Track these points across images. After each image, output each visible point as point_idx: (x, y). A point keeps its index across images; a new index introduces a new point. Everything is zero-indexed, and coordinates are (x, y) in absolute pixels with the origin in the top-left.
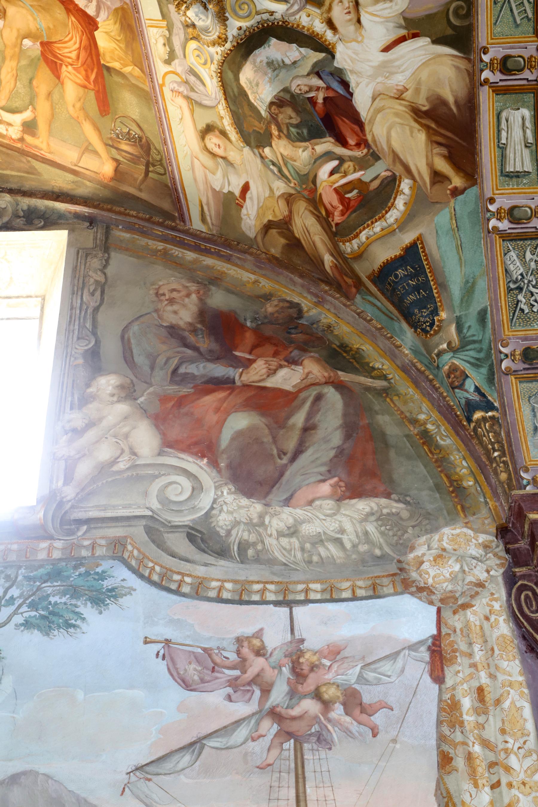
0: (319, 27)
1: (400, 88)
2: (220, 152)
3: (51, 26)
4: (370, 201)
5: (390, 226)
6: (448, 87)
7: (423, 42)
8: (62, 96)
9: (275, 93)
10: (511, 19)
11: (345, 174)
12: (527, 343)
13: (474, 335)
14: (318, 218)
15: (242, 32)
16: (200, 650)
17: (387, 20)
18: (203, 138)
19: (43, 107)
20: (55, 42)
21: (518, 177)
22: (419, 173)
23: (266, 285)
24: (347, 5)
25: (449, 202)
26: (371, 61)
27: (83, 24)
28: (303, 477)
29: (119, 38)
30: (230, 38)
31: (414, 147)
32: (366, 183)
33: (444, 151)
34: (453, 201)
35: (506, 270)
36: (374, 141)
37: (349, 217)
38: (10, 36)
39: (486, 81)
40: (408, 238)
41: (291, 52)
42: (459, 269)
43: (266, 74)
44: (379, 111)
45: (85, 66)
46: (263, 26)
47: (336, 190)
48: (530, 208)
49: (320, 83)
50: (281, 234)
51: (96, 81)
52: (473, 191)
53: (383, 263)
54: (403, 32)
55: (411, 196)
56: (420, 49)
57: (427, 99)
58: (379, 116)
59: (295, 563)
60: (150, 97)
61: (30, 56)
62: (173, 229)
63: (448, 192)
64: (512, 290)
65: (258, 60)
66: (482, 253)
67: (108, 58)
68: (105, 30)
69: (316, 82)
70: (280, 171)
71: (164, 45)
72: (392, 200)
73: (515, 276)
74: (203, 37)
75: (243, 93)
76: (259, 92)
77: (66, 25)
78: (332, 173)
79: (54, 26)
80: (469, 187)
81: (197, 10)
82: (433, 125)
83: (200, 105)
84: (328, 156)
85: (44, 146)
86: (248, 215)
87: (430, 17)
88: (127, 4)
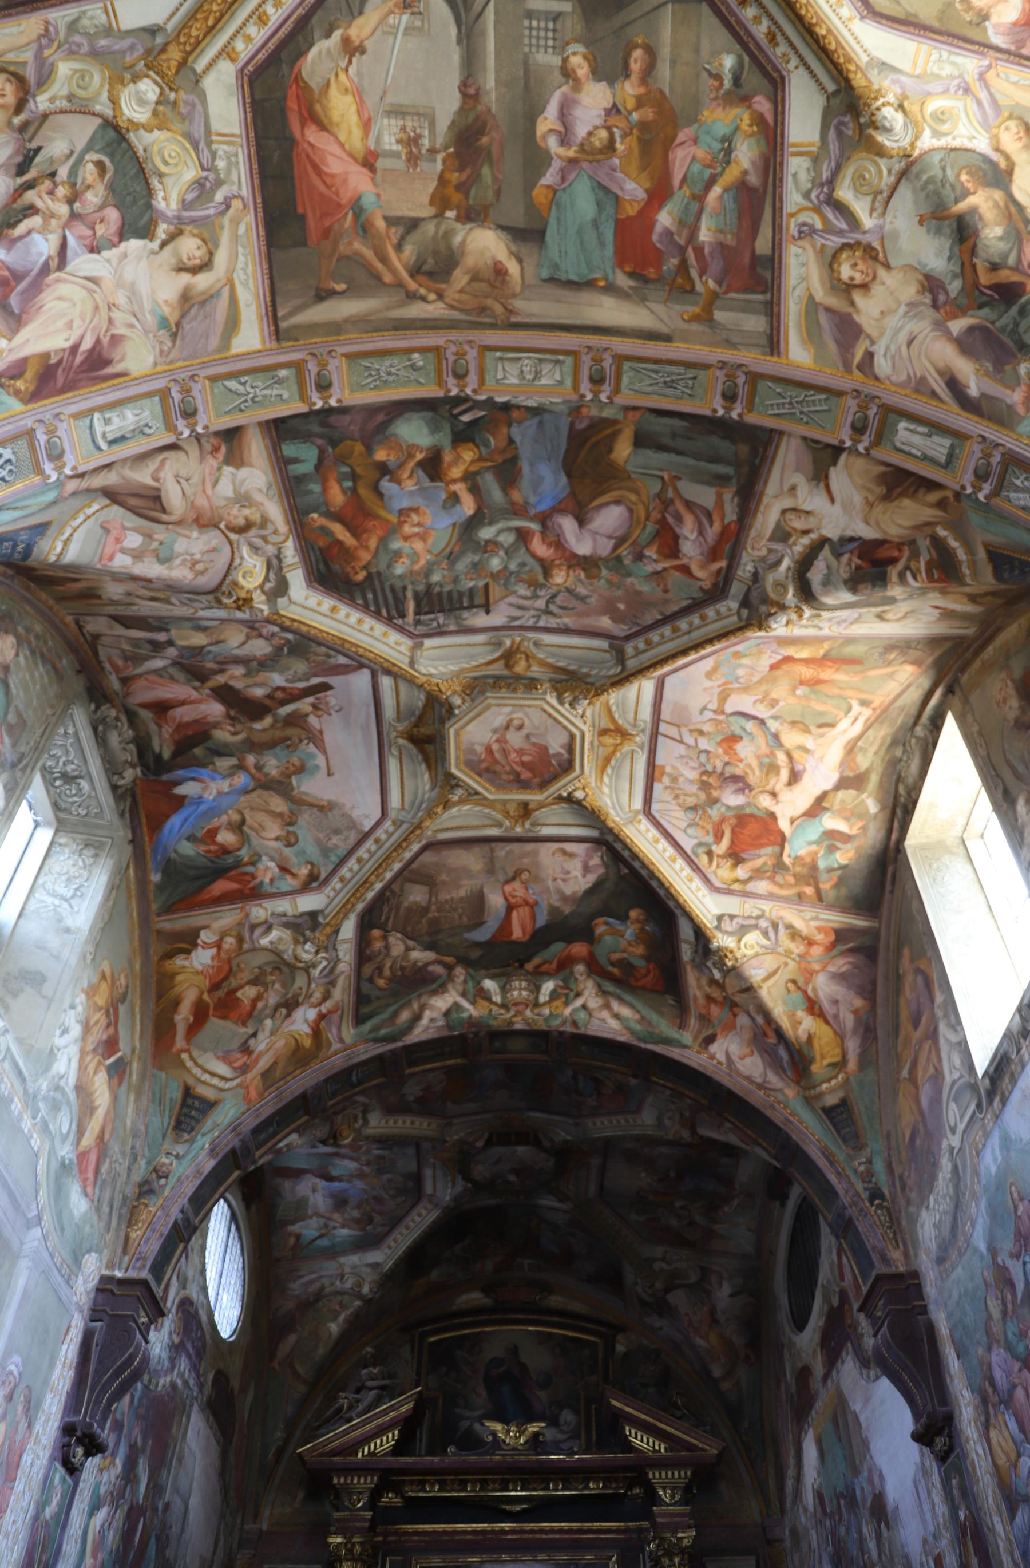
0: (805, 541)
19: (848, 693)
54: (822, 485)
85: (881, 699)
87: (815, 462)
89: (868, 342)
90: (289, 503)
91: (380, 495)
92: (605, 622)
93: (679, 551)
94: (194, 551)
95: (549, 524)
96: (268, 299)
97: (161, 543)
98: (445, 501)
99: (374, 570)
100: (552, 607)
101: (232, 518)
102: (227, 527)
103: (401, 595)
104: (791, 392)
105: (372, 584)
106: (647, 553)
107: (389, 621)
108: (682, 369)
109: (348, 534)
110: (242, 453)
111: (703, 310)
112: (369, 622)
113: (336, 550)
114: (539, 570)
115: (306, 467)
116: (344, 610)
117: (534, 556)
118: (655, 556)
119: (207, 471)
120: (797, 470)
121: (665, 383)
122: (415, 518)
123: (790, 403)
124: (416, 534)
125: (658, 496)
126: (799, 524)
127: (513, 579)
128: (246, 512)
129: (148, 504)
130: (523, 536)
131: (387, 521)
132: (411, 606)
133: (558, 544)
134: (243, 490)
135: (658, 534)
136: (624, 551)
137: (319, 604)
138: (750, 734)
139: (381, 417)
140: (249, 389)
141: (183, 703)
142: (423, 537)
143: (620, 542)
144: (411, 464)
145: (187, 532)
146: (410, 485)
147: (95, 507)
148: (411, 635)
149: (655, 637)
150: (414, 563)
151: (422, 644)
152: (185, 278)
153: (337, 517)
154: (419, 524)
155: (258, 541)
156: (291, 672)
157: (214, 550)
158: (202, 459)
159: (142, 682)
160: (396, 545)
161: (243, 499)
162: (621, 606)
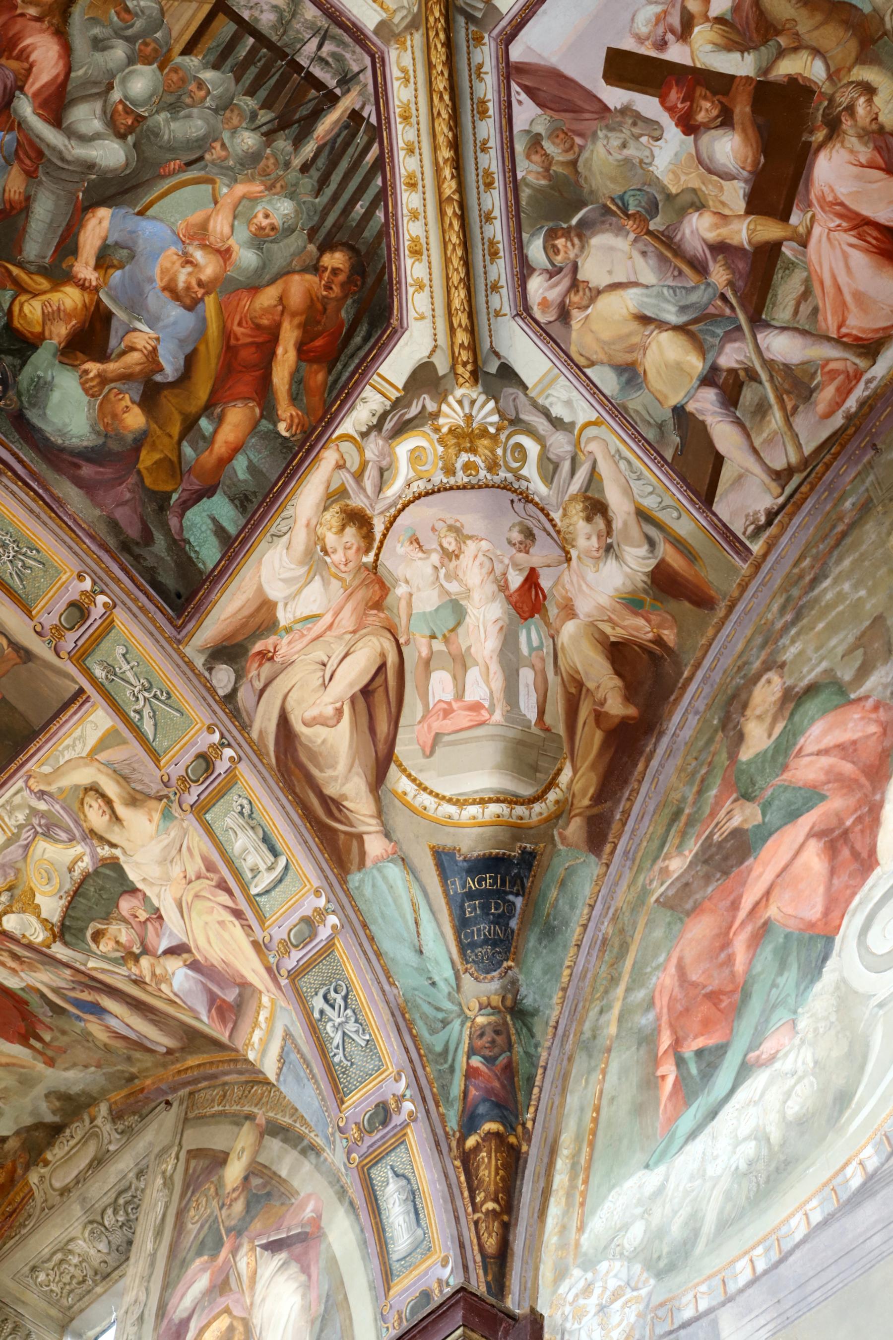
90: (285, 485)
91: (190, 360)
94: (429, 570)
96: (75, 707)
97: (433, 637)
98: (121, 267)
99: (312, 248)
101: (351, 553)
102: (367, 551)
103: (321, 162)
105: (338, 226)
107: (379, 132)
109: (280, 351)
110: (252, 615)
112: (406, 165)
113: (319, 343)
115: (221, 507)
116: (410, 230)
119: (299, 646)
122: (183, 277)
124: (204, 247)
128: (331, 539)
129: (380, 699)
131: (220, 310)
132: (328, 123)
134: (304, 570)
137: (421, 287)
139: (87, 470)
140: (141, 702)
141: (860, 224)
142: (200, 234)
144: (112, 367)
145: (403, 604)
146: (143, 336)
147: (404, 785)
148: (378, 63)
150: (254, 200)
151: (382, 26)
152: (121, 810)
153: (263, 391)
154: (188, 261)
155: (369, 482)
156: (631, 152)
157: (415, 541)
158: (287, 665)
159: (858, 323)
160: (246, 258)
161: (316, 557)
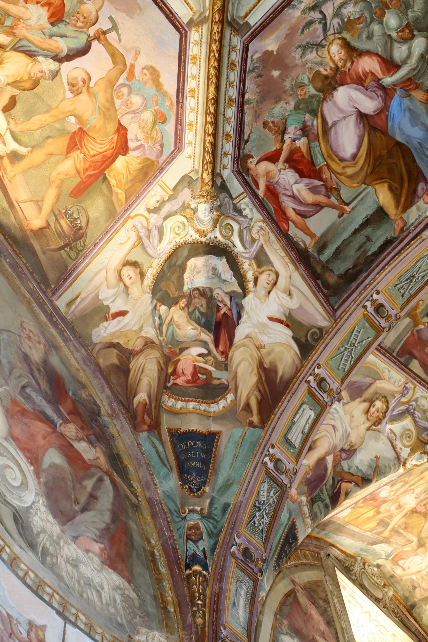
0: (250, 276)
1: (263, 344)
2: (127, 282)
3: (98, 127)
4: (207, 389)
5: (209, 412)
6: (283, 366)
7: (289, 333)
8: (57, 163)
9: (204, 286)
10: (338, 363)
11: (206, 363)
12: (249, 546)
13: (216, 515)
14: (161, 370)
15: (215, 240)
16: (4, 612)
17: (282, 305)
18: (124, 265)
20: (90, 136)
21: (290, 445)
22: (240, 397)
23: (83, 377)
24: (270, 280)
25: (245, 426)
26: (259, 317)
27: (118, 145)
28: (85, 528)
29: (132, 172)
30: (208, 237)
31: (247, 381)
32: (212, 377)
33: (259, 397)
34: (247, 427)
35: (259, 492)
36: (231, 359)
37: (190, 387)
38: (66, 106)
39: (308, 382)
40: (214, 427)
41: (228, 274)
42: (228, 469)
43: (208, 272)
44: (244, 345)
45: (93, 164)
46: (226, 248)
47: (195, 366)
48: (286, 467)
49: (228, 303)
50: (119, 358)
51: (89, 176)
52: (259, 431)
53: (193, 430)
54: (284, 319)
55: (230, 405)
56: (284, 335)
57: (270, 362)
58: (243, 348)
59: (73, 590)
60: (115, 216)
61: (65, 126)
62: (44, 293)
63: (248, 421)
64: (256, 506)
65: (210, 261)
66: (245, 470)
67: (112, 174)
68: (128, 160)
69: (227, 300)
70: (161, 325)
71: (158, 202)
72: (218, 399)
73: (260, 500)
74: (196, 222)
75: (183, 268)
76: (196, 277)
77: (107, 135)
78: (200, 355)
79: (100, 129)
80: (259, 428)
81: (208, 208)
82: (263, 378)
83: (144, 248)
84: (205, 344)
86: (106, 328)
87: (300, 324)
88: (159, 163)
89: (345, 401)
92: (270, 43)
93: (290, 167)
95: (380, 93)
100: (316, 15)
104: (360, 349)
106: (304, 140)
108: (412, 292)
111: (416, 314)
114: (355, 43)
117: (368, 53)
118: (298, 143)
120: (301, 307)
121: (414, 277)
123: (354, 346)
125: (337, 190)
126: (264, 279)
127: (366, 14)
130: (390, 65)
133: (360, 81)
135: (312, 163)
136: (317, 123)
138: (51, 36)
143: (326, 129)
149: (234, 76)
162: (276, 73)
